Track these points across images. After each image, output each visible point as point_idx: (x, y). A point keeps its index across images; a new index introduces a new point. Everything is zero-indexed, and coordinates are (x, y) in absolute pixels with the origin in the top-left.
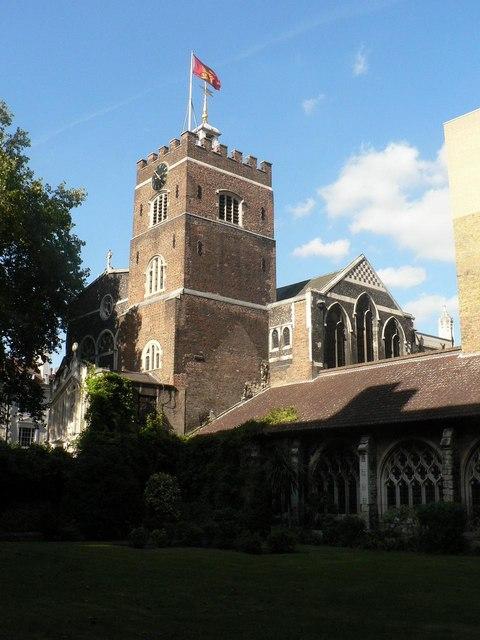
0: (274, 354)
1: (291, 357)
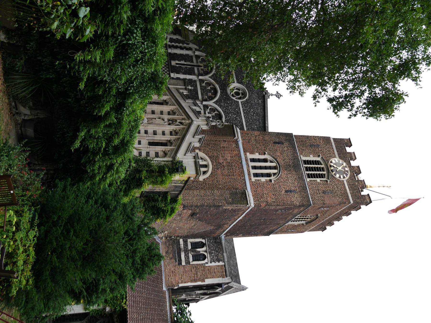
0: (185, 242)
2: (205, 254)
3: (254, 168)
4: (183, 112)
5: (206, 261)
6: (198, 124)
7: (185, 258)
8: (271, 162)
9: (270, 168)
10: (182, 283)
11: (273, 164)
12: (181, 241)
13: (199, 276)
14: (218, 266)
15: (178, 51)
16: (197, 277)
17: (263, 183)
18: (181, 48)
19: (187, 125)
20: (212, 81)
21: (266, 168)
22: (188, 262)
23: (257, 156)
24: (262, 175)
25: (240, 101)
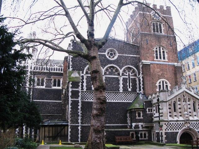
3: (160, 58)
6: (185, 88)
8: (157, 49)
9: (160, 50)
15: (85, 84)
17: (168, 56)
18: (83, 82)
20: (106, 67)
21: (160, 52)
23: (155, 55)
24: (164, 55)
25: (117, 55)
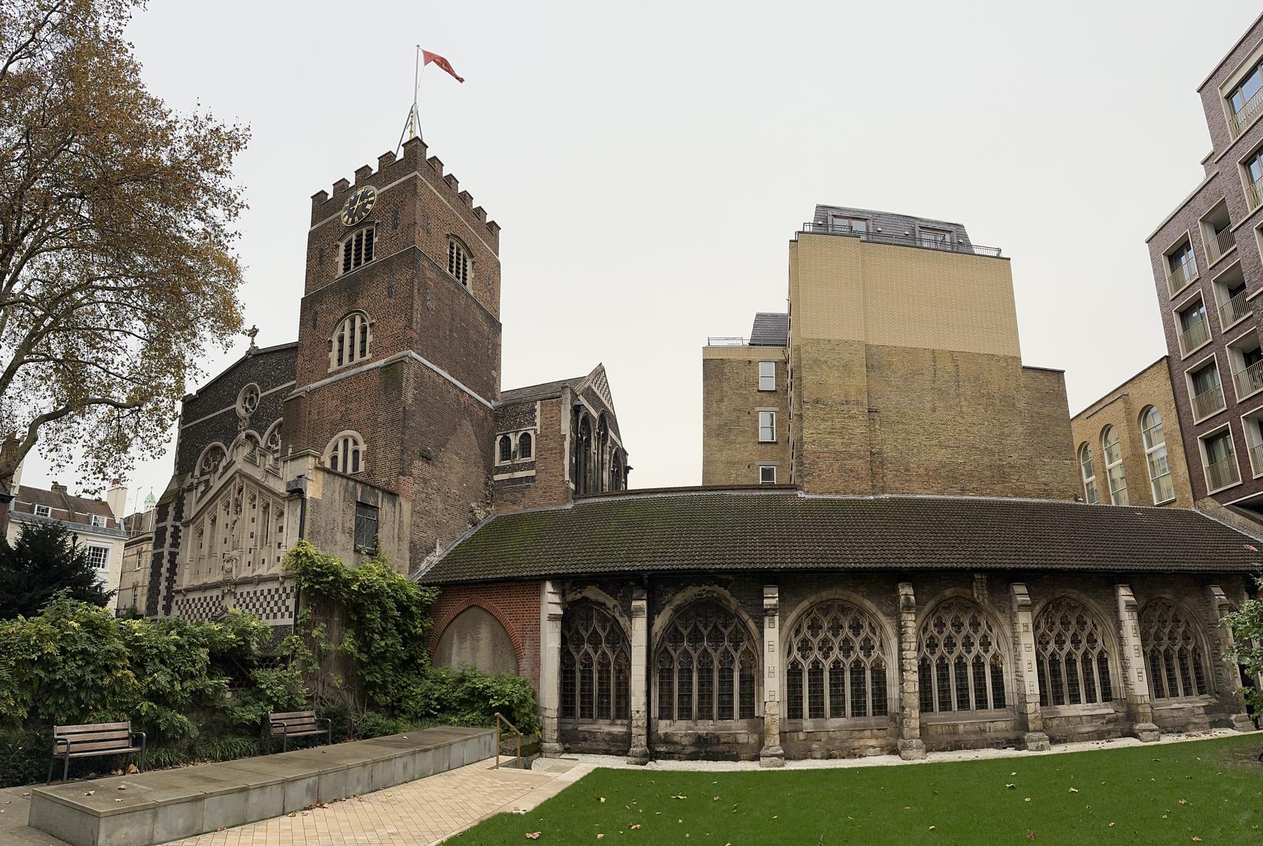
1: (533, 473)
2: (520, 434)
4: (226, 488)
5: (531, 433)
6: (242, 461)
7: (525, 470)
9: (353, 329)
10: (563, 476)
11: (347, 323)
12: (497, 478)
13: (555, 445)
14: (542, 411)
16: (556, 448)
19: (243, 479)
21: (352, 337)
22: (531, 466)
23: (334, 355)
24: (363, 342)
